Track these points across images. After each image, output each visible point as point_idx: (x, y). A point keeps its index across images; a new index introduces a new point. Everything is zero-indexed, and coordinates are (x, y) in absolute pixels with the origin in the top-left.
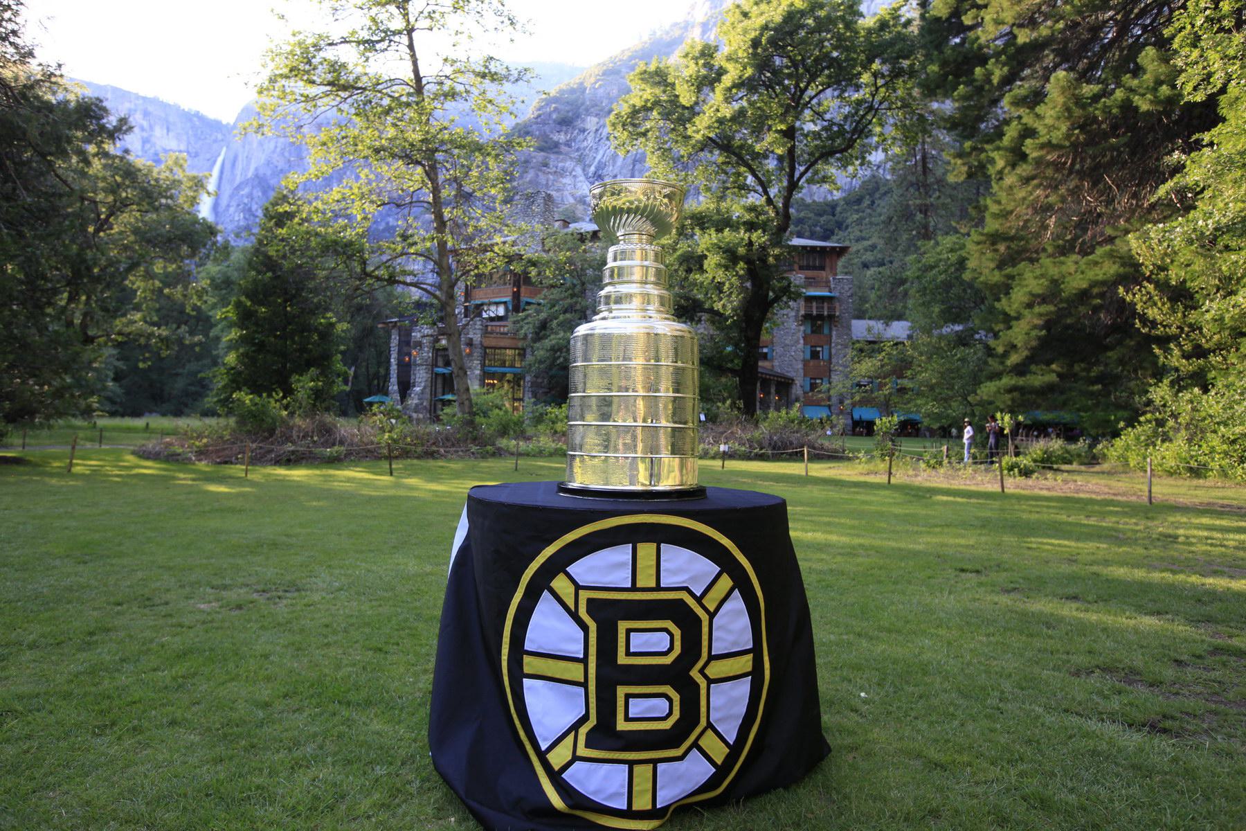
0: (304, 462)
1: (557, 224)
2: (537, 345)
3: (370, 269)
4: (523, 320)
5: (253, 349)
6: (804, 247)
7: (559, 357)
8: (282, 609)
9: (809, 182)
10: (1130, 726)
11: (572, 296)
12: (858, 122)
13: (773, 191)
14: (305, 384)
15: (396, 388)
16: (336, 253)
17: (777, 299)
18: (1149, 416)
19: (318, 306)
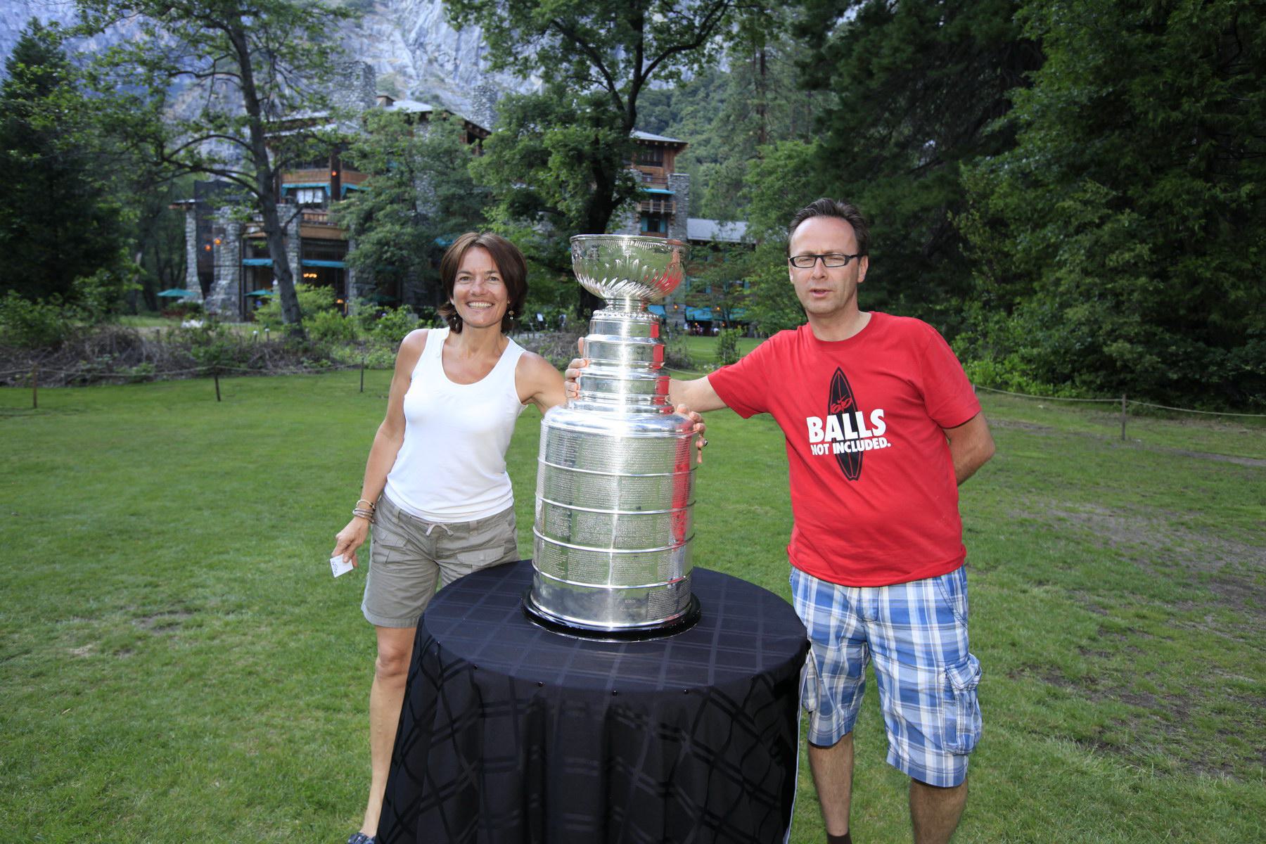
0: (104, 382)
1: (379, 101)
2: (363, 238)
3: (167, 151)
4: (345, 208)
5: (11, 235)
6: (643, 141)
7: (386, 252)
8: (181, 643)
9: (656, 77)
10: (1079, 741)
11: (400, 184)
12: (708, 17)
13: (619, 86)
14: (92, 287)
15: (195, 279)
16: (126, 135)
17: (621, 201)
18: (963, 335)
19: (99, 192)
